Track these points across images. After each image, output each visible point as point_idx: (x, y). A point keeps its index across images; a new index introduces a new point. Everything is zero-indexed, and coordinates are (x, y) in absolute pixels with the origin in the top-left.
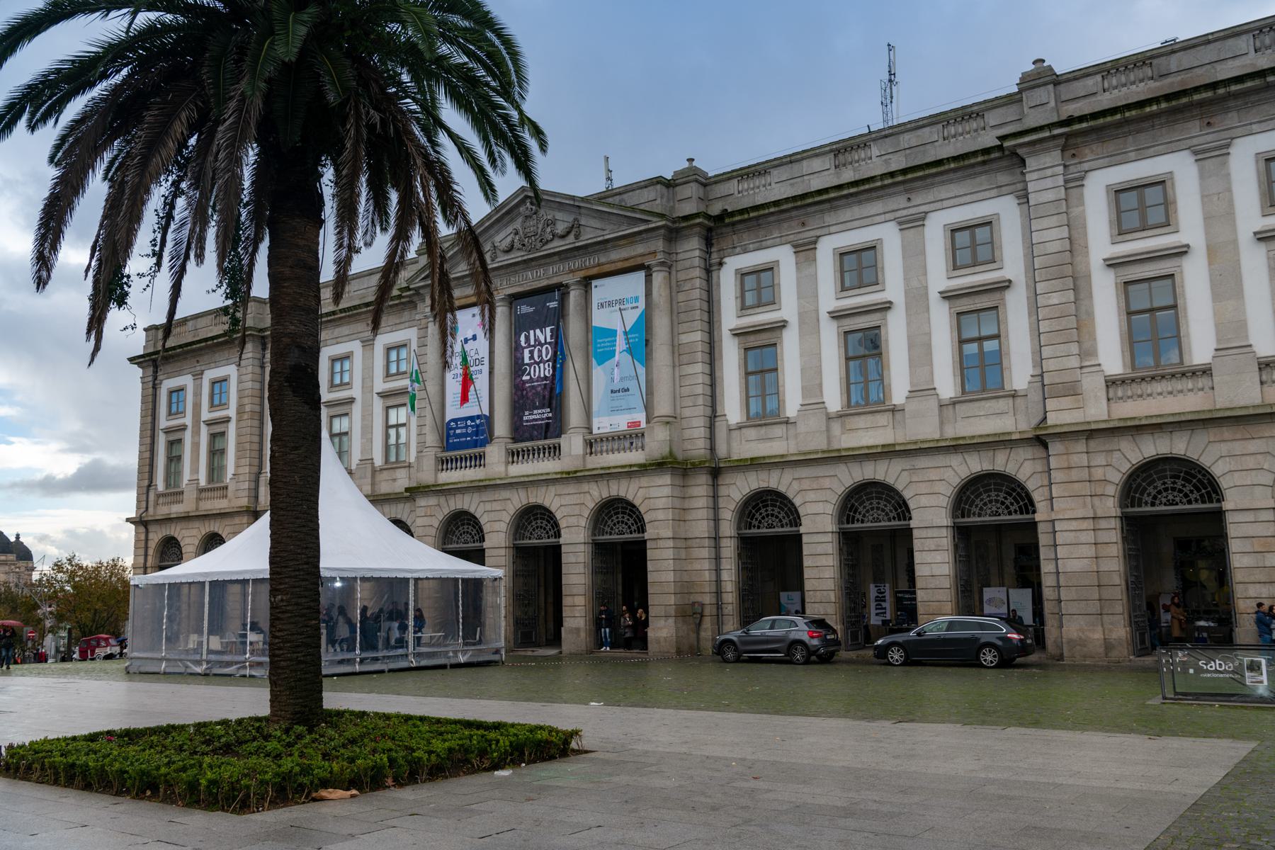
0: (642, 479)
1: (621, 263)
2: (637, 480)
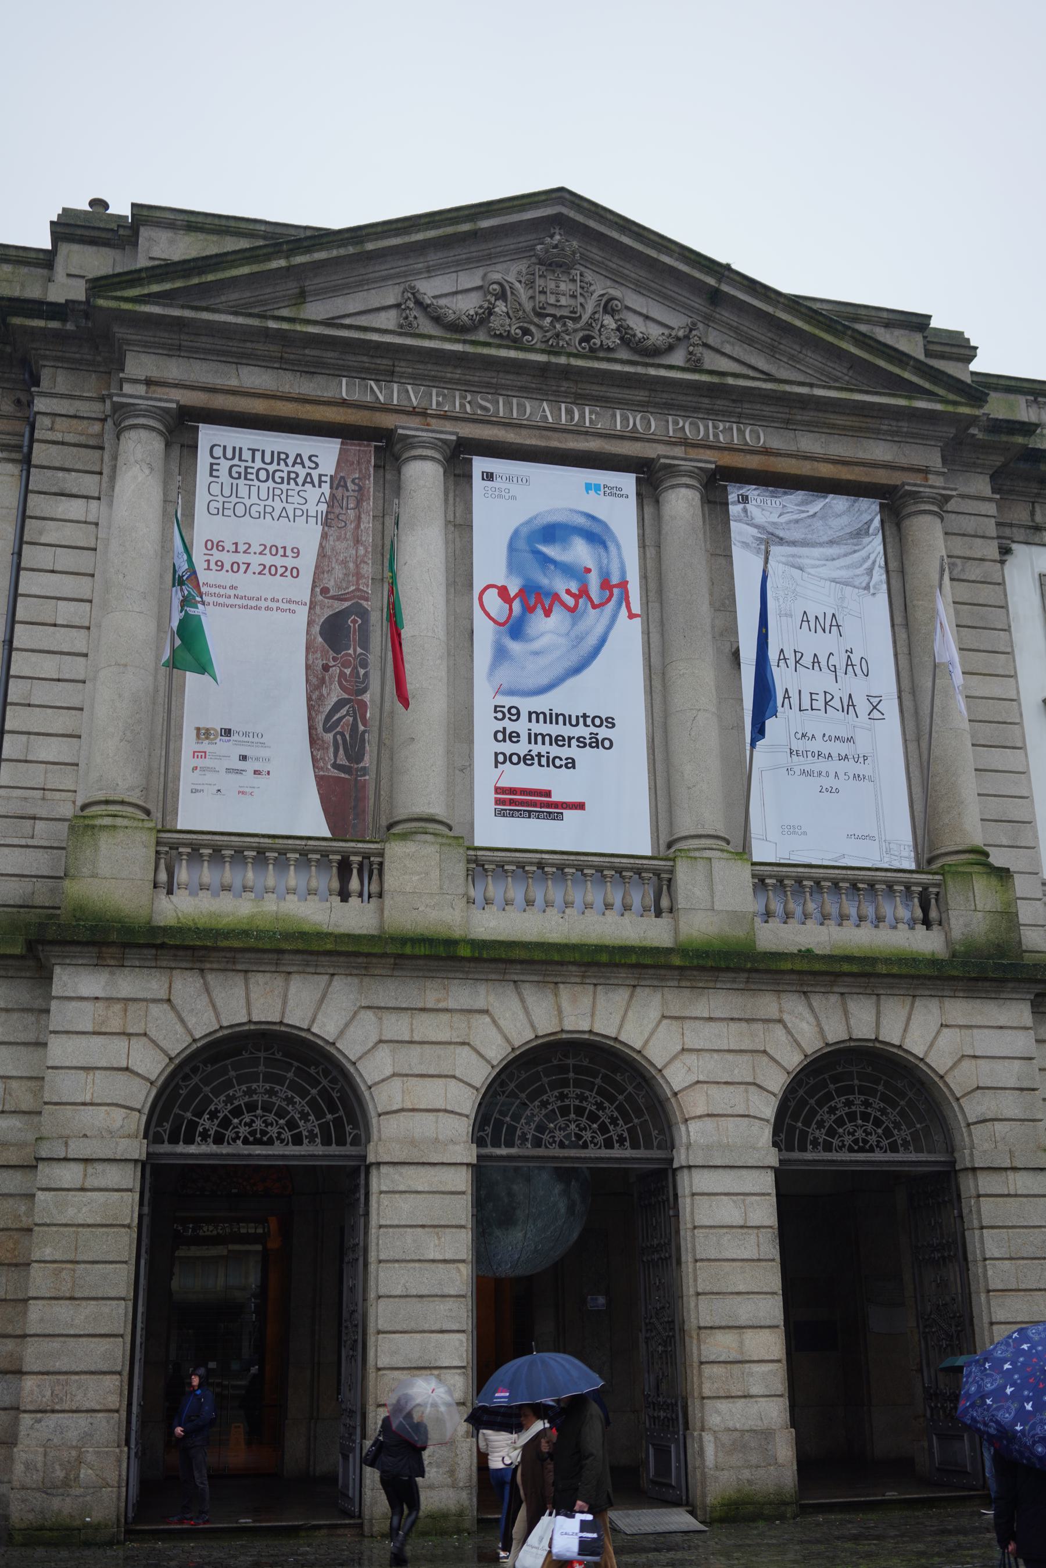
0: (948, 1003)
1: (831, 466)
2: (933, 1005)
